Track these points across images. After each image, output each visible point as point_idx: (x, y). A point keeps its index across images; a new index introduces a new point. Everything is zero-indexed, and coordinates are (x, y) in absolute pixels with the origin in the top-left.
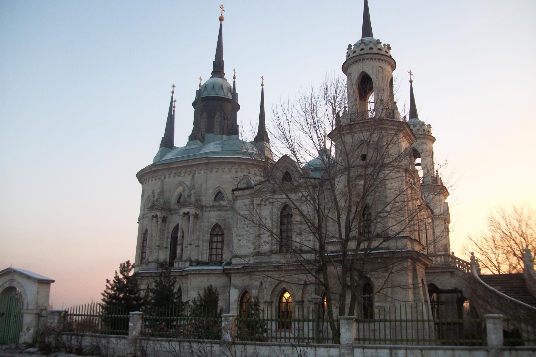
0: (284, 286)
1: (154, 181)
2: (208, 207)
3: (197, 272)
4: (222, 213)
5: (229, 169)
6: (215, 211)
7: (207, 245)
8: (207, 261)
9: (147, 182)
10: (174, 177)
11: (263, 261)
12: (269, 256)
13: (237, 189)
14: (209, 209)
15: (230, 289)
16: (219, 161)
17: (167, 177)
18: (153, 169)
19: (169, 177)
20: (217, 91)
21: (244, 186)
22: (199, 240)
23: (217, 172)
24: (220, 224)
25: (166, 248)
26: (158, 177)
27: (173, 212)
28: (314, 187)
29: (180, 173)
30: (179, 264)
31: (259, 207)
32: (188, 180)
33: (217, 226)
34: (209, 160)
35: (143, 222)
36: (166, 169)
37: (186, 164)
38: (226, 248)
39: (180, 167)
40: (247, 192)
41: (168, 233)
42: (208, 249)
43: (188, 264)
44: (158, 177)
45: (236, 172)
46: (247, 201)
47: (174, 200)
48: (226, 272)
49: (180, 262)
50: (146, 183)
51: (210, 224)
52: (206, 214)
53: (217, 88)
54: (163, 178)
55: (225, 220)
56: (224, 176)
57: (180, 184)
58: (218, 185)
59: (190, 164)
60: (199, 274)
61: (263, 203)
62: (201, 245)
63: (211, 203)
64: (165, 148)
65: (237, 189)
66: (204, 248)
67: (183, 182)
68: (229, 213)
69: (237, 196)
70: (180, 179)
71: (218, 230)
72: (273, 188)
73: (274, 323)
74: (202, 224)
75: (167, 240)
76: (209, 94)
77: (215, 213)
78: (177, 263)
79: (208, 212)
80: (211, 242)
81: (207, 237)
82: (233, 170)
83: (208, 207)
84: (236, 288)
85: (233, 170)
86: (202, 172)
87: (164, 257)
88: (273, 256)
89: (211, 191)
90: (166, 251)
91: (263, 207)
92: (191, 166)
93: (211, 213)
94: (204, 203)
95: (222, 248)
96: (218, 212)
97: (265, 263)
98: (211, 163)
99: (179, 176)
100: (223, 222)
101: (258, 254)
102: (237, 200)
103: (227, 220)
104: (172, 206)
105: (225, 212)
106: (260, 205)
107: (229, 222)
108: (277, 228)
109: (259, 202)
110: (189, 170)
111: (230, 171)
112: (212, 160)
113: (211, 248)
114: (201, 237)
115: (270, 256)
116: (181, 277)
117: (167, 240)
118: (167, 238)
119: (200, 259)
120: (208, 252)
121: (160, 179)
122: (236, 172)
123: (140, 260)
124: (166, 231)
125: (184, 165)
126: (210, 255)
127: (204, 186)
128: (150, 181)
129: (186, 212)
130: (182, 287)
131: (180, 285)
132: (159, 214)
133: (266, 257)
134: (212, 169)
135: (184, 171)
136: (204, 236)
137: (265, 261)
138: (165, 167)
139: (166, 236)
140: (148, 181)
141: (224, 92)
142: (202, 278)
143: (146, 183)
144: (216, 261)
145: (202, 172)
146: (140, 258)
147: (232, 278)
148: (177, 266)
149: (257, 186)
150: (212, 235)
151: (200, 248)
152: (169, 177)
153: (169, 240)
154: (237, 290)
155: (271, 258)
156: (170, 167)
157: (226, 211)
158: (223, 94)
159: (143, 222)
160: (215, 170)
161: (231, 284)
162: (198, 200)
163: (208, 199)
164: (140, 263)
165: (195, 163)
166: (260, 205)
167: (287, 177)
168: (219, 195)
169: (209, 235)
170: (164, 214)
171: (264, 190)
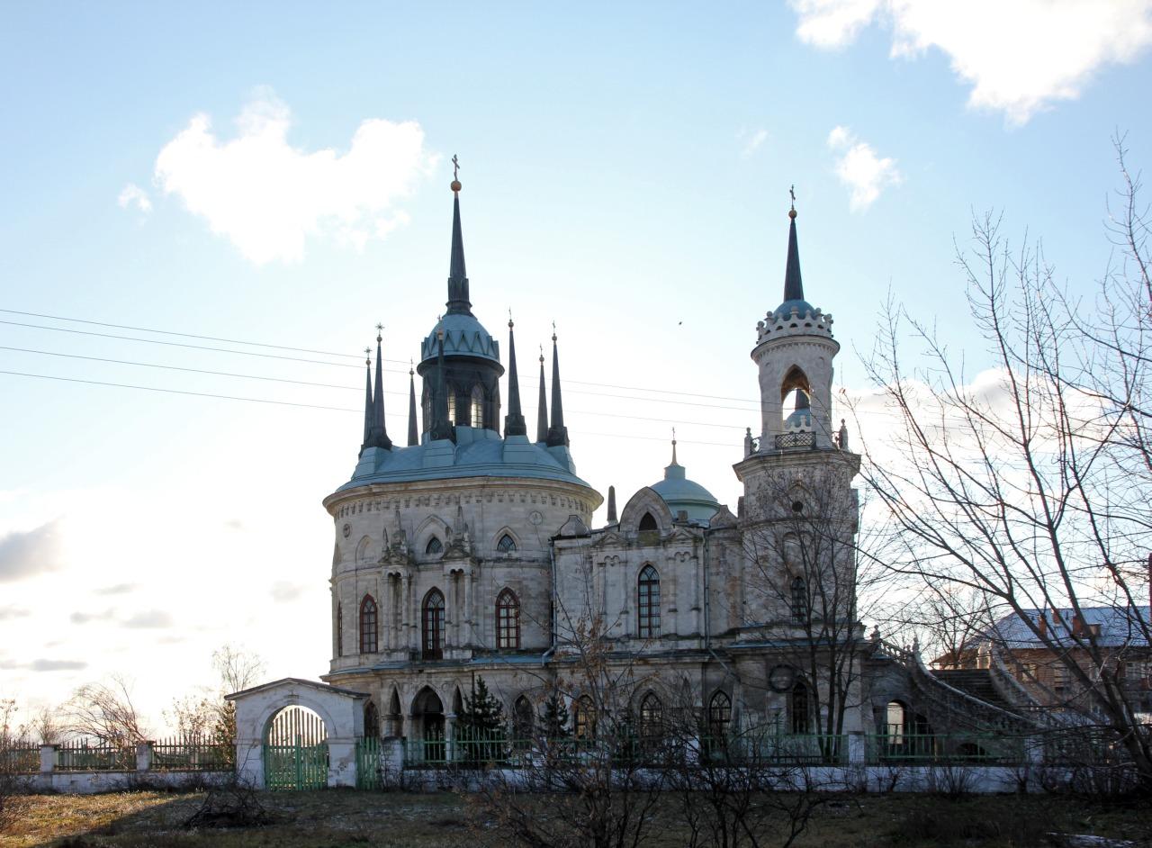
0: (650, 687)
2: (489, 561)
3: (496, 668)
4: (515, 570)
5: (523, 497)
6: (501, 567)
7: (491, 622)
8: (495, 648)
10: (417, 505)
12: (623, 643)
13: (560, 537)
14: (491, 564)
16: (505, 483)
17: (402, 505)
18: (374, 491)
19: (407, 506)
20: (470, 345)
21: (573, 533)
22: (477, 614)
23: (501, 501)
24: (513, 589)
25: (415, 627)
26: (386, 505)
27: (421, 567)
28: (696, 539)
29: (429, 500)
30: (452, 653)
31: (601, 568)
32: (448, 514)
33: (507, 591)
34: (488, 481)
35: (357, 582)
36: (399, 492)
37: (443, 486)
38: (526, 627)
39: (429, 490)
40: (581, 542)
41: (416, 602)
42: (494, 629)
43: (468, 654)
44: (382, 505)
45: (534, 502)
46: (579, 558)
47: (420, 547)
48: (550, 666)
49: (454, 652)
50: (353, 512)
51: (494, 588)
52: (486, 571)
53: (469, 338)
54: (393, 506)
55: (520, 582)
56: (514, 509)
57: (433, 519)
58: (504, 524)
59: (450, 485)
60: (498, 669)
61: (608, 561)
62: (481, 622)
63: (495, 555)
64: (380, 449)
65: (560, 537)
66: (488, 628)
67: (436, 516)
68: (526, 570)
69: (560, 549)
70: (431, 510)
71: (507, 598)
72: (627, 539)
74: (481, 588)
75: (415, 614)
76: (457, 351)
77: (502, 570)
79: (489, 570)
80: (498, 618)
81: (492, 609)
82: (529, 499)
83: (489, 561)
85: (529, 499)
86: (473, 500)
87: (413, 641)
88: (632, 642)
89: (492, 534)
90: (415, 632)
91: (608, 567)
92: (451, 488)
93: (494, 569)
94: (481, 554)
95: (517, 628)
96: (508, 570)
97: (616, 653)
98: (490, 486)
99: (427, 505)
100: (518, 586)
102: (561, 555)
103: (525, 583)
104: (419, 558)
105: (520, 570)
106: (601, 564)
107: (527, 586)
108: (634, 602)
109: (602, 561)
110: (446, 494)
111: (523, 501)
112: (494, 480)
113: (499, 628)
114: (481, 610)
115: (626, 644)
116: (458, 675)
117: (415, 614)
118: (415, 610)
119: (481, 645)
120: (494, 633)
121: (388, 508)
122: (534, 502)
123: (358, 646)
124: (412, 598)
125: (439, 486)
126: (499, 638)
127: (478, 525)
129: (457, 570)
130: (461, 690)
131: (458, 690)
132: (403, 571)
133: (619, 644)
134: (492, 495)
135: (435, 496)
136: (486, 608)
137: (619, 650)
138: (398, 489)
139: (412, 606)
141: (482, 348)
142: (503, 676)
143: (353, 512)
144: (508, 647)
145: (473, 500)
150: (499, 607)
151: (481, 628)
152: (407, 506)
153: (419, 614)
155: (627, 647)
156: (410, 488)
157: (522, 567)
158: (480, 351)
159: (357, 582)
160: (495, 499)
162: (473, 549)
163: (487, 548)
164: (359, 651)
165: (461, 485)
168: (506, 541)
169: (494, 607)
170: (410, 572)
171: (610, 541)
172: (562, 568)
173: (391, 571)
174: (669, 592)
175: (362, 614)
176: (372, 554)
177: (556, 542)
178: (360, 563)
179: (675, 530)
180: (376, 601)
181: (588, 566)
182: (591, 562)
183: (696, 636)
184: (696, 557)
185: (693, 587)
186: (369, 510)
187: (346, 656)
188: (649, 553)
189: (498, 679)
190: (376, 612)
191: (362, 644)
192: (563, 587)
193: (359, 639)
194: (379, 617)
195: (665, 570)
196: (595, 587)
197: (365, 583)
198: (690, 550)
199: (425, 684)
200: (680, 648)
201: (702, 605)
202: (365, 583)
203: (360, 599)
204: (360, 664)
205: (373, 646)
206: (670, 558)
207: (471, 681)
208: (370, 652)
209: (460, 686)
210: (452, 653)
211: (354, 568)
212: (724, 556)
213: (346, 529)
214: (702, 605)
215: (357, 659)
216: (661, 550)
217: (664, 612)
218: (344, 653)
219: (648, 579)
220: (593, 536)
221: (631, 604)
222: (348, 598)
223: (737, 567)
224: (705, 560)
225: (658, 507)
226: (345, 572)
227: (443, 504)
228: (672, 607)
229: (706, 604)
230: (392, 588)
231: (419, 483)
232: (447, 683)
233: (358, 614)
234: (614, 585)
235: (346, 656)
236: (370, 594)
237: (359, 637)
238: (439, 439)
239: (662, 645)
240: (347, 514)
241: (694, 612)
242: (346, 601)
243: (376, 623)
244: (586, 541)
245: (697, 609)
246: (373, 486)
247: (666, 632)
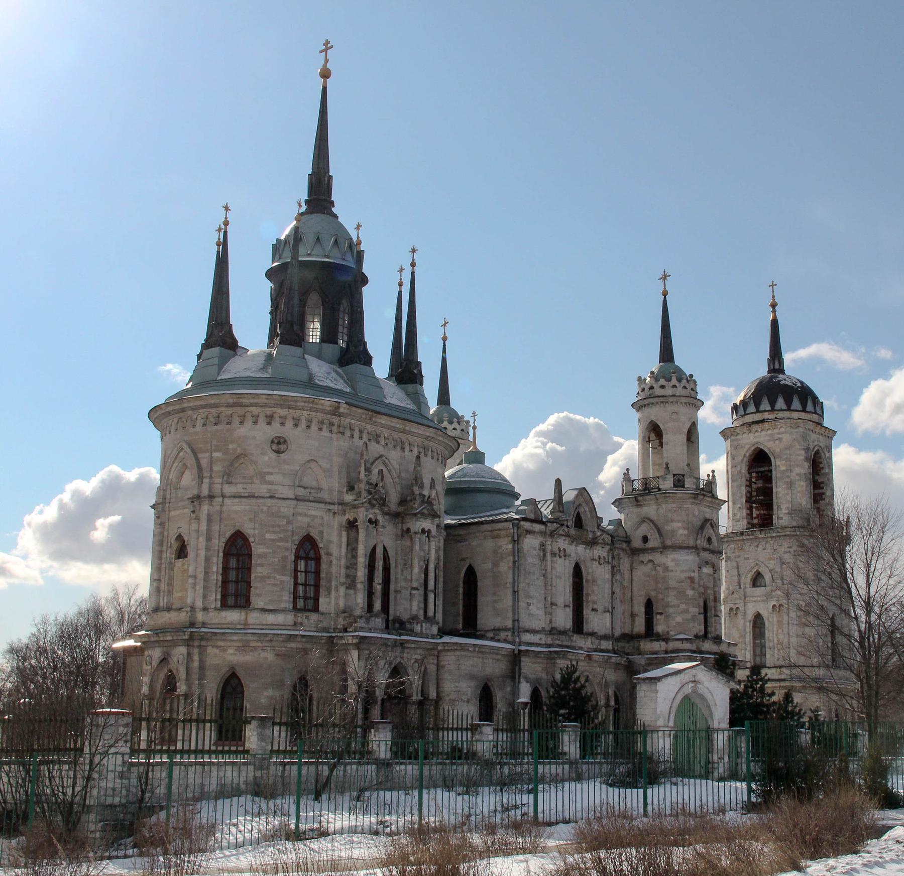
1: (325, 433)
9: (303, 424)
11: (564, 643)
15: (519, 682)
18: (342, 410)
23: (433, 458)
26: (341, 429)
30: (422, 626)
40: (538, 527)
49: (424, 624)
50: (296, 425)
54: (348, 433)
73: (526, 733)
78: (419, 625)
84: (527, 682)
99: (378, 442)
101: (553, 631)
121: (343, 433)
123: (292, 600)
128: (314, 427)
129: (427, 530)
130: (428, 671)
131: (426, 668)
140: (308, 427)
143: (296, 425)
146: (292, 596)
147: (522, 664)
148: (419, 631)
149: (555, 524)
154: (529, 684)
161: (522, 675)
166: (553, 554)
167: (579, 523)
172: (525, 551)
173: (371, 516)
174: (593, 591)
175: (297, 558)
176: (314, 484)
177: (522, 523)
178: (301, 492)
179: (599, 534)
180: (321, 545)
181: (542, 554)
182: (544, 550)
183: (605, 637)
184: (608, 562)
185: (607, 591)
186: (320, 429)
187: (264, 610)
188: (578, 551)
189: (471, 662)
190: (318, 559)
191: (295, 598)
192: (525, 570)
193: (292, 590)
194: (324, 566)
195: (590, 570)
196: (549, 576)
197: (306, 520)
198: (605, 554)
199: (399, 660)
200: (602, 648)
201: (610, 610)
202: (306, 520)
203: (297, 538)
204: (295, 624)
205: (310, 604)
206: (595, 560)
207: (436, 661)
208: (305, 610)
209: (428, 666)
210: (422, 626)
211: (294, 497)
212: (619, 563)
213: (279, 443)
214: (610, 610)
215: (289, 618)
216: (588, 551)
217: (587, 612)
218: (257, 601)
219: (577, 572)
220: (549, 524)
221: (571, 599)
222: (274, 532)
223: (627, 575)
224: (613, 567)
225: (587, 509)
226: (271, 497)
227: (391, 446)
228: (595, 606)
229: (613, 608)
230: (344, 534)
231: (384, 417)
232: (416, 661)
233: (293, 558)
234: (560, 578)
235: (264, 610)
236: (312, 534)
237: (292, 587)
238: (364, 364)
239: (592, 643)
240: (283, 424)
241: (608, 614)
242: (268, 536)
243: (317, 573)
244: (542, 527)
245: (608, 611)
246: (345, 405)
247: (590, 630)
